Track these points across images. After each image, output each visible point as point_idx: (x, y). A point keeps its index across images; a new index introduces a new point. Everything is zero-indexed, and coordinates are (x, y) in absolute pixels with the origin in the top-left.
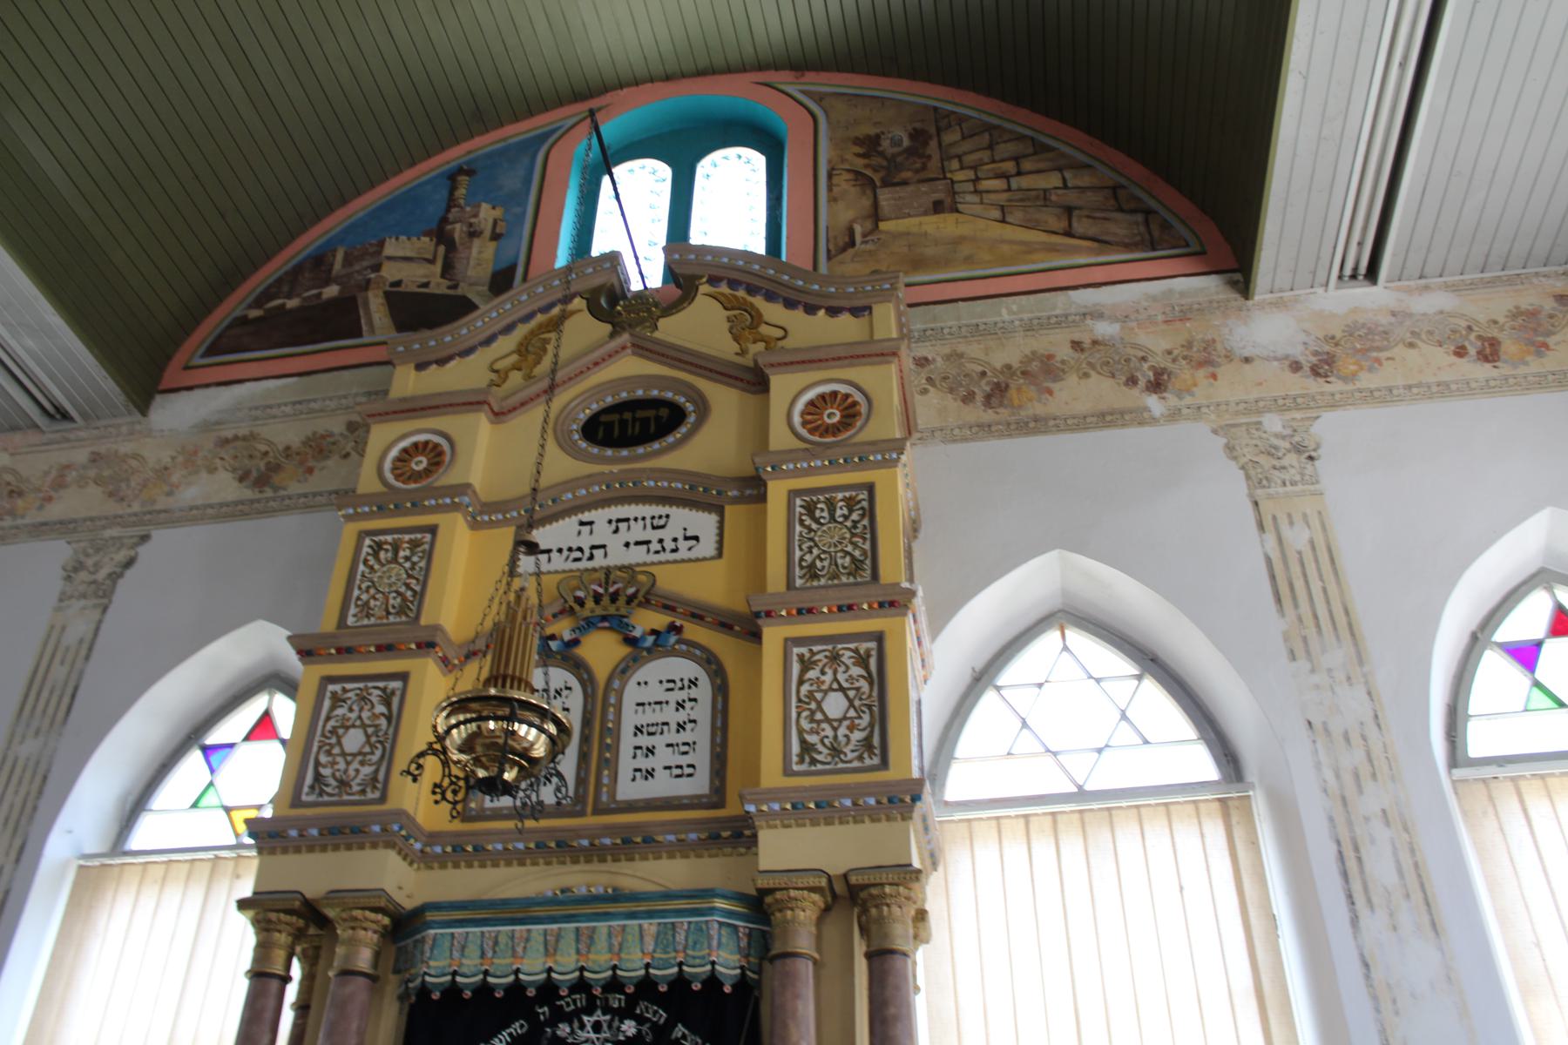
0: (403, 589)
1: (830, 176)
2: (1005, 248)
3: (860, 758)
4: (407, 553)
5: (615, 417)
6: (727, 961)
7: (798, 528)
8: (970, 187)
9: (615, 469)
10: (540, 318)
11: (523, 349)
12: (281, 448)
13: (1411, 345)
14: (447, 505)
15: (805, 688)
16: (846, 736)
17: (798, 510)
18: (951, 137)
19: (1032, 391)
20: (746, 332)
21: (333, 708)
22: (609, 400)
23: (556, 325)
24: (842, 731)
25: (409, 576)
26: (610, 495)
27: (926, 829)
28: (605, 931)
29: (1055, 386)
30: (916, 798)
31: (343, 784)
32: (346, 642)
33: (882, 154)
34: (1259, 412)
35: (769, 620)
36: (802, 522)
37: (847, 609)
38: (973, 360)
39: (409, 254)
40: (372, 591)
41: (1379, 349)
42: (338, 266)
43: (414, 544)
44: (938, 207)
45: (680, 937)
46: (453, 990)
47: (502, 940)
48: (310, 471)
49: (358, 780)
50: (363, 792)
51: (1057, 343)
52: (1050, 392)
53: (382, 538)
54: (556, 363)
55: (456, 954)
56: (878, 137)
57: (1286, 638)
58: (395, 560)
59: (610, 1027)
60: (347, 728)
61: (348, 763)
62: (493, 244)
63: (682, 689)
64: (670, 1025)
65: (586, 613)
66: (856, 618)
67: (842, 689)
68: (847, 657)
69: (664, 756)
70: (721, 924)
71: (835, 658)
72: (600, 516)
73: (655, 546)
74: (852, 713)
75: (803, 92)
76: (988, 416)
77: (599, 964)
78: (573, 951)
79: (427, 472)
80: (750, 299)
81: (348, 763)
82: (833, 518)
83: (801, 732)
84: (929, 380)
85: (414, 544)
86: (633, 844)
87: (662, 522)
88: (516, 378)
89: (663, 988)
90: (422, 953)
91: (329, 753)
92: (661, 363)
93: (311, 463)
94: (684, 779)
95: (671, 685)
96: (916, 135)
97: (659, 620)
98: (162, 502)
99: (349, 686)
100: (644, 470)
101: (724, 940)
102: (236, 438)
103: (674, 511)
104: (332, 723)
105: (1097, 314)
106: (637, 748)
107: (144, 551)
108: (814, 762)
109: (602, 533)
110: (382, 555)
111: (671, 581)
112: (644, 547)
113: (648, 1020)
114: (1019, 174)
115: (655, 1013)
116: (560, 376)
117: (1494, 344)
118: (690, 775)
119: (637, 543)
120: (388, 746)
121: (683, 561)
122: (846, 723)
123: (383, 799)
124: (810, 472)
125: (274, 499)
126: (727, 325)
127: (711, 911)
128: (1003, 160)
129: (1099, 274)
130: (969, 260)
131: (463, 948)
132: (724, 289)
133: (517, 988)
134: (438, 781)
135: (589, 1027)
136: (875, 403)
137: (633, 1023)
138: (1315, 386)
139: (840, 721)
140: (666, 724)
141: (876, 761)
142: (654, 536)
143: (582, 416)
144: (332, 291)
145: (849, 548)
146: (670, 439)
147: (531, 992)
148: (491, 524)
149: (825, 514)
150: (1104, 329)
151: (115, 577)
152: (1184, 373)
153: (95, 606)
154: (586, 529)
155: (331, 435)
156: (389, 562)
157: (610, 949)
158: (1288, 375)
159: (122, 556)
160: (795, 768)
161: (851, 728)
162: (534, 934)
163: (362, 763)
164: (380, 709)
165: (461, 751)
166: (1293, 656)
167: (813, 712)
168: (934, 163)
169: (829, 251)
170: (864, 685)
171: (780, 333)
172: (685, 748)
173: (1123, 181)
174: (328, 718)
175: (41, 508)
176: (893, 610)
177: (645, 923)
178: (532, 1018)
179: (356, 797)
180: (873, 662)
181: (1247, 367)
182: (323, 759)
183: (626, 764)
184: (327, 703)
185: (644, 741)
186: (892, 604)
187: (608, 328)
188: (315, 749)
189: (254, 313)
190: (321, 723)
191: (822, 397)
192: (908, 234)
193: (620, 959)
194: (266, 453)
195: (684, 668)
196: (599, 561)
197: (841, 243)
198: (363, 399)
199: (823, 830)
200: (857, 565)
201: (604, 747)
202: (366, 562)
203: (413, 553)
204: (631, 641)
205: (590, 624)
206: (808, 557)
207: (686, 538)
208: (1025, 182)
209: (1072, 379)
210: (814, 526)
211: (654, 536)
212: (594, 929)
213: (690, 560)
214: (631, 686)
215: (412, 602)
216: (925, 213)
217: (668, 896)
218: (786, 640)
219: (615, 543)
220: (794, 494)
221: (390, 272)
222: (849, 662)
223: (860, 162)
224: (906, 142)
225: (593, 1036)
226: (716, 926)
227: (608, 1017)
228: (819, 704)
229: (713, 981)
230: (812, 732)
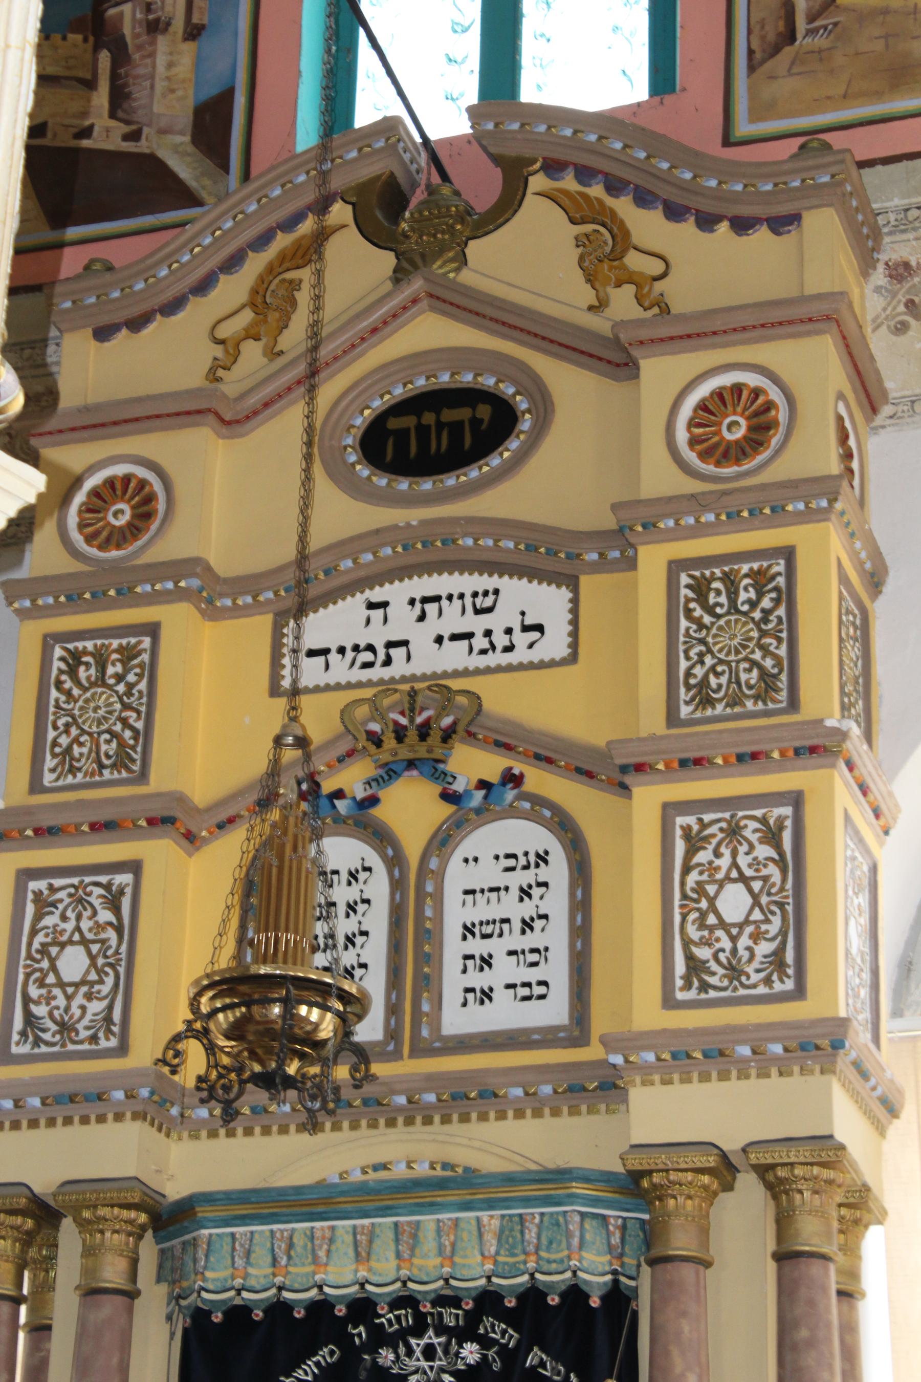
0: (118, 727)
3: (768, 981)
4: (119, 668)
5: (409, 422)
6: (594, 1269)
7: (684, 623)
9: (415, 515)
10: (282, 241)
11: (258, 300)
14: (168, 592)
15: (693, 878)
16: (749, 949)
17: (684, 592)
20: (606, 266)
21: (38, 917)
22: (399, 392)
23: (311, 251)
24: (744, 941)
25: (126, 707)
26: (411, 559)
27: (864, 1075)
28: (432, 1226)
30: (837, 1045)
31: (66, 1028)
32: (47, 821)
35: (641, 777)
36: (688, 612)
37: (751, 758)
40: (74, 731)
46: (238, 1314)
47: (299, 1241)
49: (85, 1022)
50: (94, 1039)
53: (80, 645)
54: (312, 389)
55: (239, 1262)
58: (101, 681)
59: (446, 1352)
60: (63, 945)
61: (69, 998)
63: (526, 867)
64: (523, 1349)
65: (385, 757)
66: (764, 771)
67: (743, 879)
68: (751, 831)
69: (506, 969)
70: (583, 1215)
71: (733, 832)
72: (397, 593)
73: (480, 642)
74: (757, 915)
77: (427, 1270)
78: (391, 1255)
79: (134, 530)
80: (610, 201)
81: (69, 998)
82: (733, 607)
83: (687, 943)
84: (910, 304)
85: (128, 655)
86: (468, 1099)
87: (488, 602)
88: (252, 352)
89: (510, 1303)
90: (195, 1261)
91: (41, 983)
94: (533, 1002)
95: (511, 862)
97: (491, 765)
99: (58, 882)
100: (454, 521)
101: (588, 1236)
103: (506, 584)
104: (40, 938)
106: (467, 957)
108: (705, 987)
109: (402, 621)
110: (82, 673)
111: (503, 699)
112: (465, 643)
113: (495, 1342)
115: (504, 1332)
116: (324, 352)
118: (542, 997)
119: (455, 637)
120: (122, 970)
121: (521, 667)
122: (750, 929)
124: (700, 530)
127: (572, 1198)
131: (248, 1254)
132: (569, 183)
133: (321, 1308)
134: (202, 1072)
135: (418, 1353)
136: (800, 406)
137: (475, 1347)
139: (741, 926)
140: (507, 921)
141: (789, 985)
142: (477, 624)
143: (358, 421)
145: (757, 656)
146: (495, 461)
147: (341, 1311)
148: (237, 611)
149: (723, 599)
154: (377, 614)
156: (93, 684)
157: (441, 1251)
160: (680, 996)
161: (756, 937)
162: (339, 1232)
163: (89, 997)
164: (105, 916)
165: (228, 1037)
167: (703, 915)
169: (751, 52)
170: (773, 871)
171: (657, 267)
172: (534, 957)
174: (34, 932)
176: (815, 759)
177: (484, 1215)
178: (344, 1341)
179: (86, 1046)
180: (787, 838)
182: (34, 992)
183: (453, 980)
184: (30, 909)
185: (477, 946)
186: (813, 750)
187: (387, 260)
188: (21, 977)
190: (25, 940)
191: (719, 394)
192: (885, 11)
193: (453, 1264)
195: (528, 835)
197: (771, 37)
199: (715, 1086)
200: (768, 681)
201: (423, 958)
202: (59, 684)
203: (127, 671)
204: (449, 797)
205: (389, 774)
206: (699, 671)
207: (526, 629)
210: (707, 619)
211: (477, 624)
212: (418, 1223)
213: (531, 666)
214: (455, 864)
215: (131, 754)
217: (510, 1179)
218: (666, 806)
219: (421, 636)
220: (675, 567)
222: (754, 838)
225: (425, 1364)
226: (577, 1218)
227: (442, 1339)
228: (712, 901)
229: (575, 1294)
230: (705, 943)
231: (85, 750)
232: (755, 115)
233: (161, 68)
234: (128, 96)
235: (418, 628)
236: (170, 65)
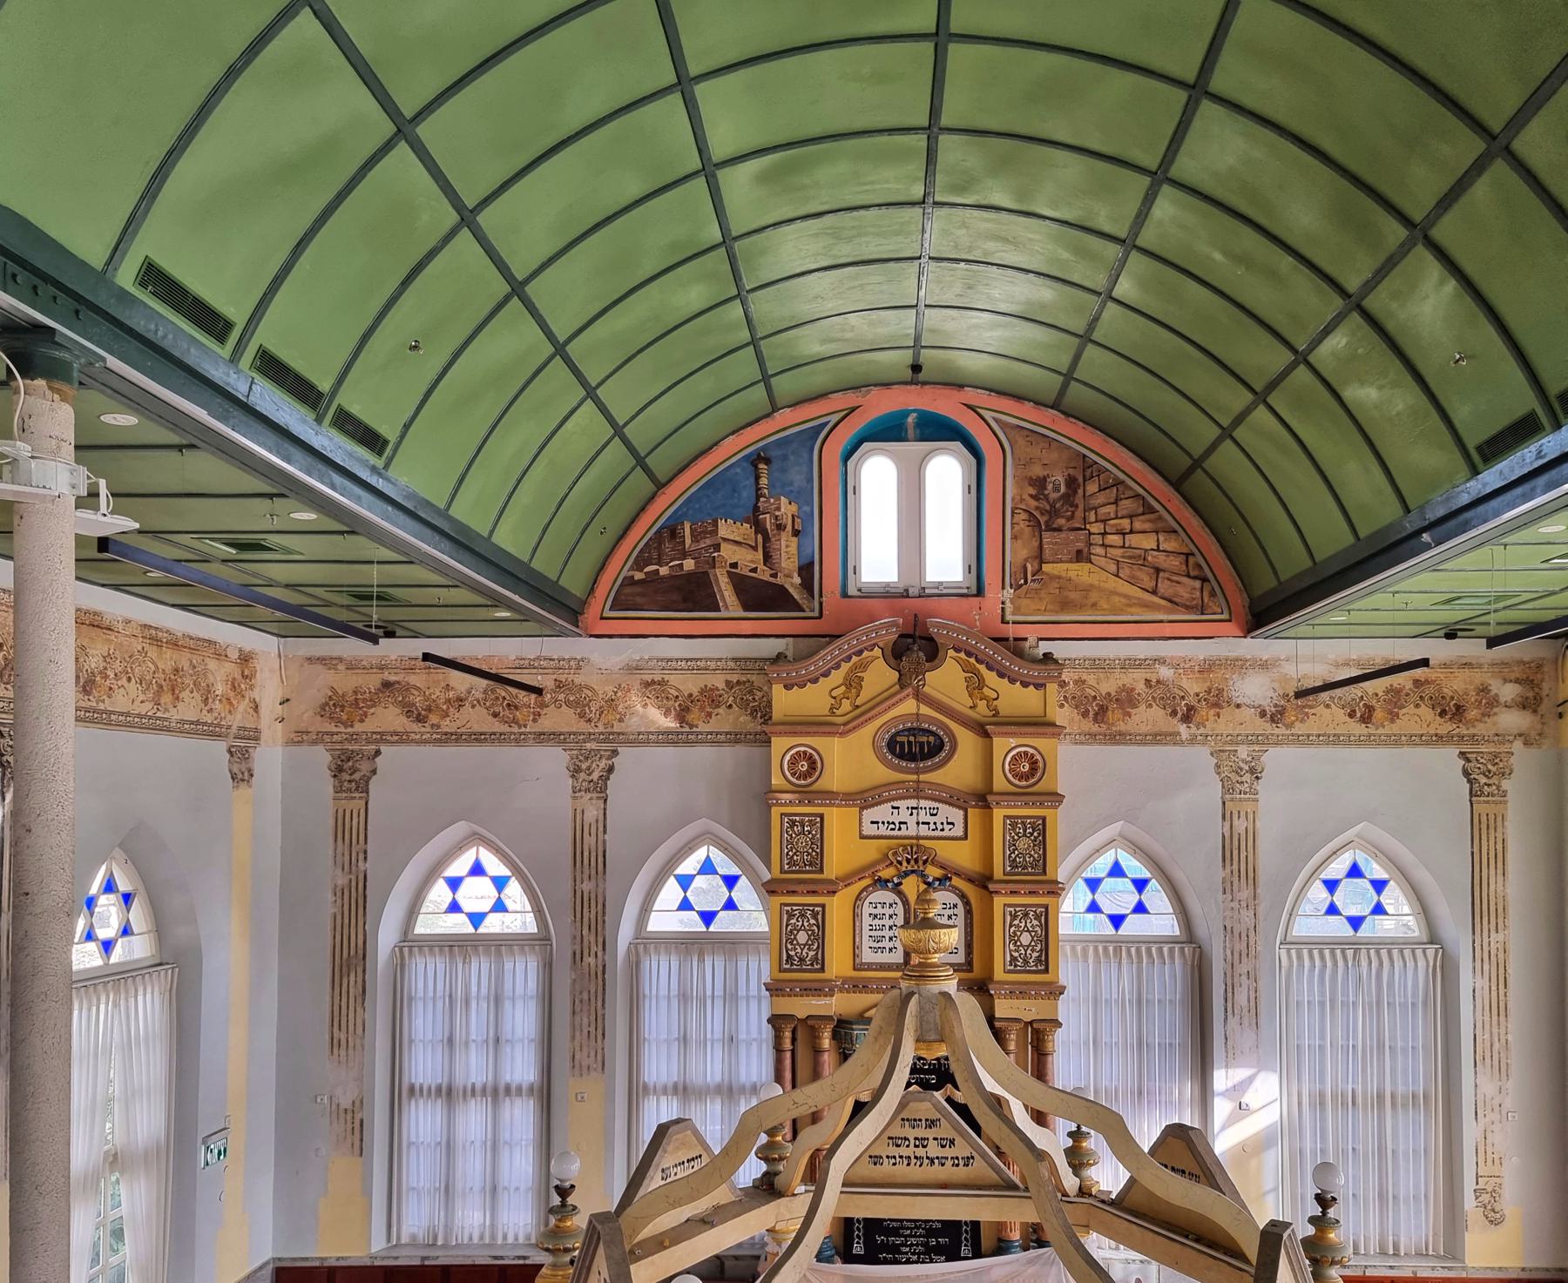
2: (1116, 599)
8: (1097, 539)
13: (1328, 706)
18: (1092, 487)
19: (1118, 714)
23: (864, 666)
29: (1133, 711)
31: (802, 960)
33: (1046, 498)
38: (1091, 687)
41: (1311, 707)
42: (688, 541)
43: (812, 824)
44: (1080, 557)
48: (709, 715)
51: (1136, 679)
56: (1045, 479)
62: (795, 539)
71: (1026, 915)
75: (996, 420)
76: (1095, 728)
88: (846, 705)
96: (1071, 482)
105: (1161, 661)
109: (904, 815)
114: (1131, 532)
117: (1370, 709)
123: (822, 970)
129: (1168, 630)
138: (1269, 728)
142: (929, 819)
144: (689, 564)
150: (1165, 673)
151: (605, 779)
152: (1204, 711)
158: (1259, 721)
168: (1079, 513)
175: (535, 720)
189: (639, 576)
196: (903, 832)
198: (732, 664)
208: (1133, 540)
211: (929, 819)
215: (818, 863)
216: (1070, 561)
221: (728, 553)
223: (1034, 503)
224: (1063, 489)
232: (1013, 614)
235: (906, 818)
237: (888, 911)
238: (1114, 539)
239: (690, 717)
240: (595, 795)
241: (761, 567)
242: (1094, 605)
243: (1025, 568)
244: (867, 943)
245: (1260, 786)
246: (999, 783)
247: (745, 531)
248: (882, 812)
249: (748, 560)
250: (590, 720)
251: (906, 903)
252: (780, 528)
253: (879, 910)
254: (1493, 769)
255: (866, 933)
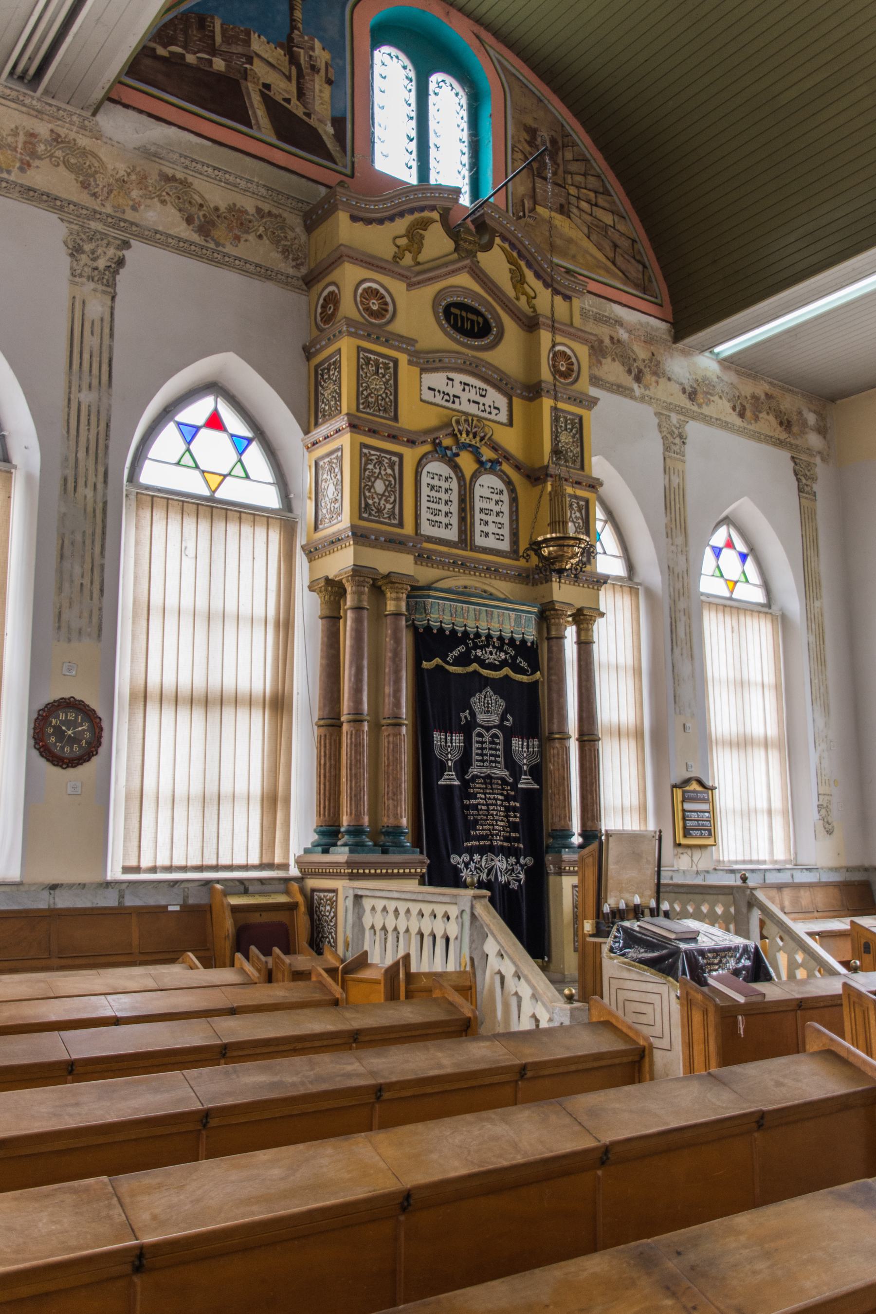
1: (513, 150)
5: (457, 311)
8: (574, 200)
12: (212, 206)
13: (721, 397)
21: (366, 464)
29: (604, 361)
34: (670, 410)
39: (270, 60)
41: (712, 395)
42: (218, 39)
43: (387, 368)
44: (563, 210)
45: (523, 622)
47: (459, 610)
48: (237, 238)
50: (389, 518)
52: (601, 363)
53: (370, 356)
57: (666, 524)
72: (458, 377)
73: (482, 408)
75: (499, 62)
81: (380, 500)
87: (484, 393)
92: (483, 288)
93: (236, 231)
98: (130, 215)
99: (373, 452)
102: (173, 179)
105: (619, 322)
107: (125, 252)
109: (457, 390)
114: (596, 205)
119: (474, 402)
125: (219, 252)
126: (509, 275)
128: (590, 190)
129: (624, 298)
130: (574, 257)
131: (443, 611)
138: (688, 404)
142: (481, 400)
144: (219, 64)
150: (623, 335)
153: (104, 292)
154: (450, 383)
155: (246, 212)
159: (111, 252)
164: (389, 471)
166: (667, 537)
173: (637, 239)
177: (511, 613)
181: (668, 383)
182: (367, 494)
184: (363, 459)
189: (161, 51)
194: (201, 206)
196: (456, 406)
198: (263, 191)
209: (609, 359)
219: (465, 396)
231: (373, 400)
233: (317, 91)
234: (304, 94)
236: (321, 91)
237: (444, 485)
238: (584, 205)
239: (216, 233)
240: (100, 287)
241: (294, 101)
242: (574, 257)
243: (523, 201)
244: (425, 515)
245: (687, 447)
246: (546, 374)
247: (276, 55)
248: (437, 379)
249: (283, 88)
250: (95, 195)
251: (461, 478)
252: (314, 69)
253: (435, 482)
254: (808, 474)
255: (424, 504)
